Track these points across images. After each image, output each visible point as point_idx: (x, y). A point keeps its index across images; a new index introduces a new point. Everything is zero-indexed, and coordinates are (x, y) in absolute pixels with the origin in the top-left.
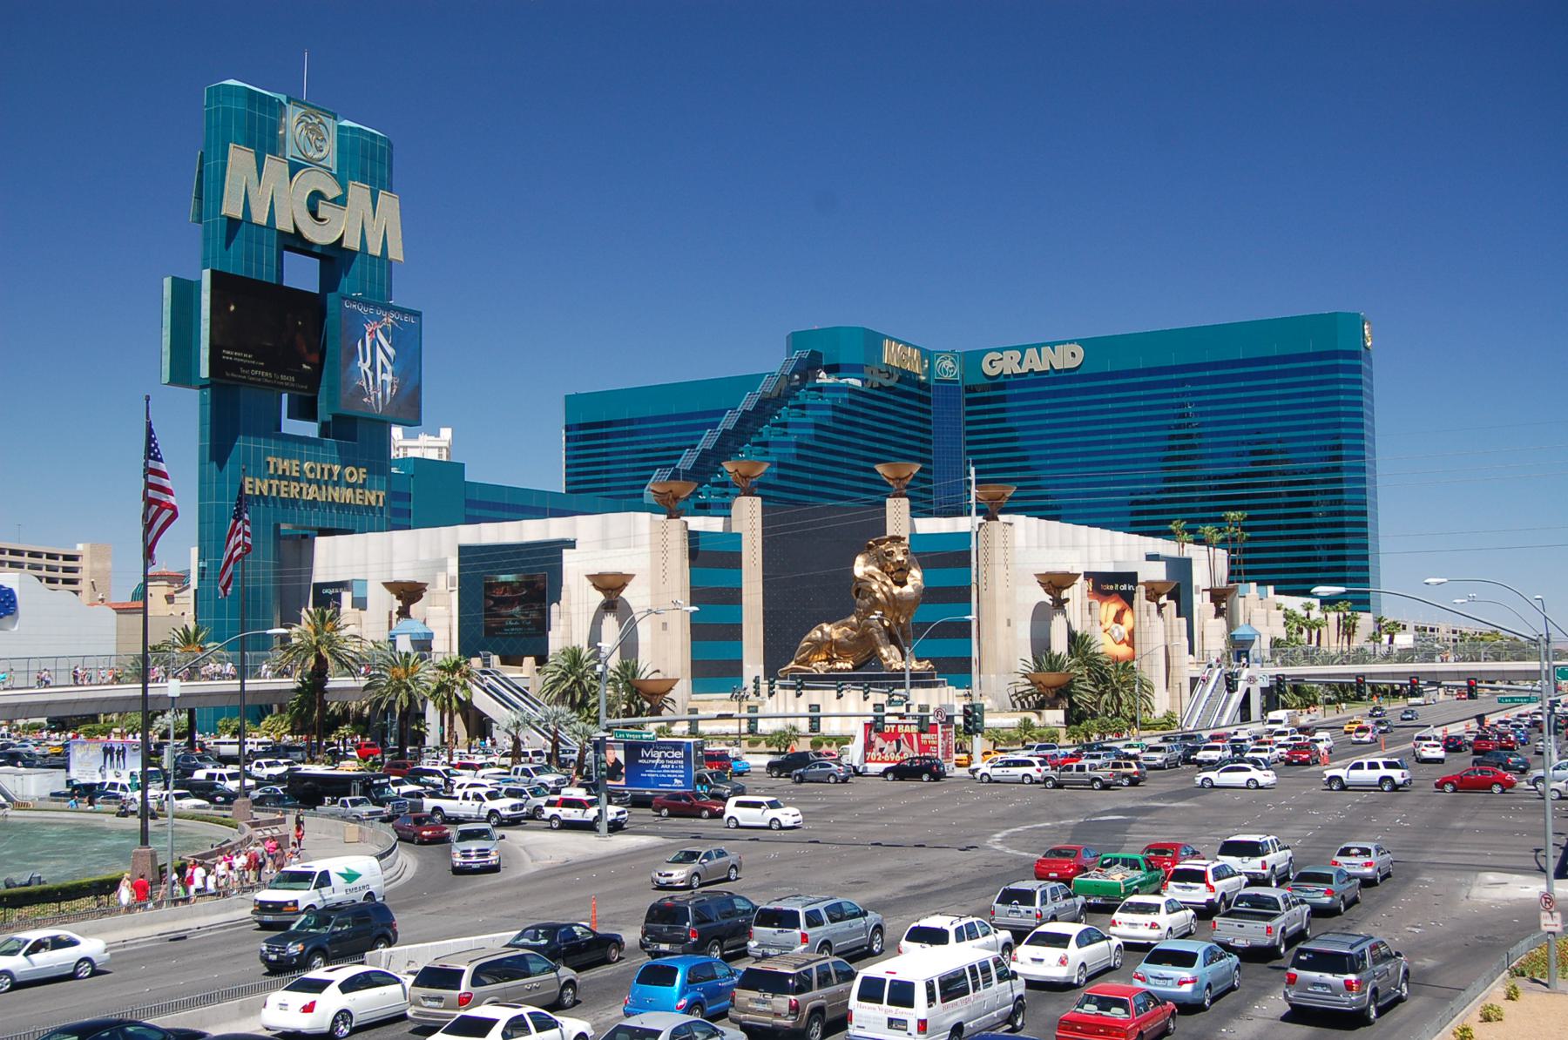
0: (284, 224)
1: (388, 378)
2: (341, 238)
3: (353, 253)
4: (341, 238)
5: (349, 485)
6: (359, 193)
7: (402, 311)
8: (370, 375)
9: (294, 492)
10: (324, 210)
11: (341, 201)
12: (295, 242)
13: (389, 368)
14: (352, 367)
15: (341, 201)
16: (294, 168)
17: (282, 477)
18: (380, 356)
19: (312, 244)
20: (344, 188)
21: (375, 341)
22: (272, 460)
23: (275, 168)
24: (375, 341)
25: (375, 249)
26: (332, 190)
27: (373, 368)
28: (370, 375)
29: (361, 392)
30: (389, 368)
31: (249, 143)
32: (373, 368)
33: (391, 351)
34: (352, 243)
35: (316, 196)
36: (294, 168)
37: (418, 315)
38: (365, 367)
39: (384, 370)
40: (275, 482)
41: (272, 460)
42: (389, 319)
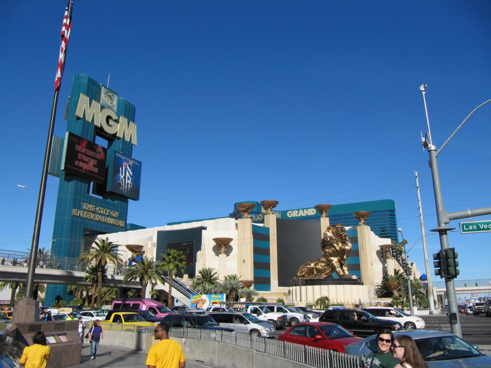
0: (97, 123)
1: (130, 182)
3: (119, 138)
6: (123, 120)
7: (136, 161)
8: (123, 180)
10: (111, 122)
11: (117, 121)
13: (130, 179)
15: (117, 121)
16: (102, 108)
18: (127, 174)
19: (106, 133)
20: (119, 117)
21: (126, 169)
24: (126, 169)
25: (127, 139)
26: (115, 117)
27: (125, 177)
28: (123, 180)
29: (120, 185)
30: (130, 179)
31: (87, 95)
32: (125, 177)
33: (131, 173)
35: (108, 118)
36: (102, 108)
37: (140, 163)
39: (128, 179)
42: (131, 163)
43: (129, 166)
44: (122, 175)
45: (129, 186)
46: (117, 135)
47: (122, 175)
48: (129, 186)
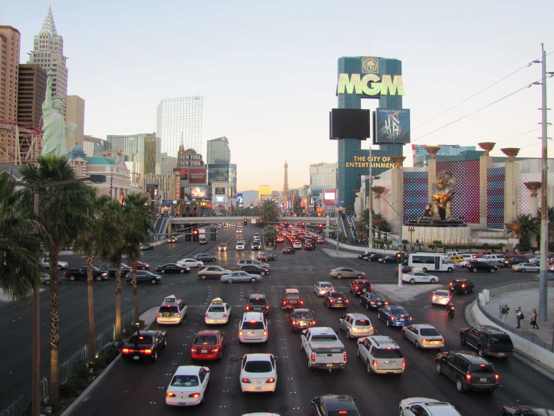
1: (397, 130)
2: (380, 92)
4: (380, 92)
5: (383, 162)
6: (386, 78)
8: (390, 130)
9: (363, 165)
11: (380, 81)
12: (365, 96)
14: (383, 128)
17: (359, 161)
18: (394, 124)
22: (355, 157)
23: (356, 77)
27: (391, 127)
28: (390, 130)
29: (386, 135)
30: (398, 127)
31: (346, 72)
32: (391, 127)
33: (398, 122)
34: (384, 92)
38: (387, 127)
39: (395, 127)
40: (356, 163)
41: (355, 157)
42: (397, 113)
43: (396, 117)
44: (388, 126)
45: (397, 133)
46: (381, 94)
47: (388, 126)
48: (397, 133)
